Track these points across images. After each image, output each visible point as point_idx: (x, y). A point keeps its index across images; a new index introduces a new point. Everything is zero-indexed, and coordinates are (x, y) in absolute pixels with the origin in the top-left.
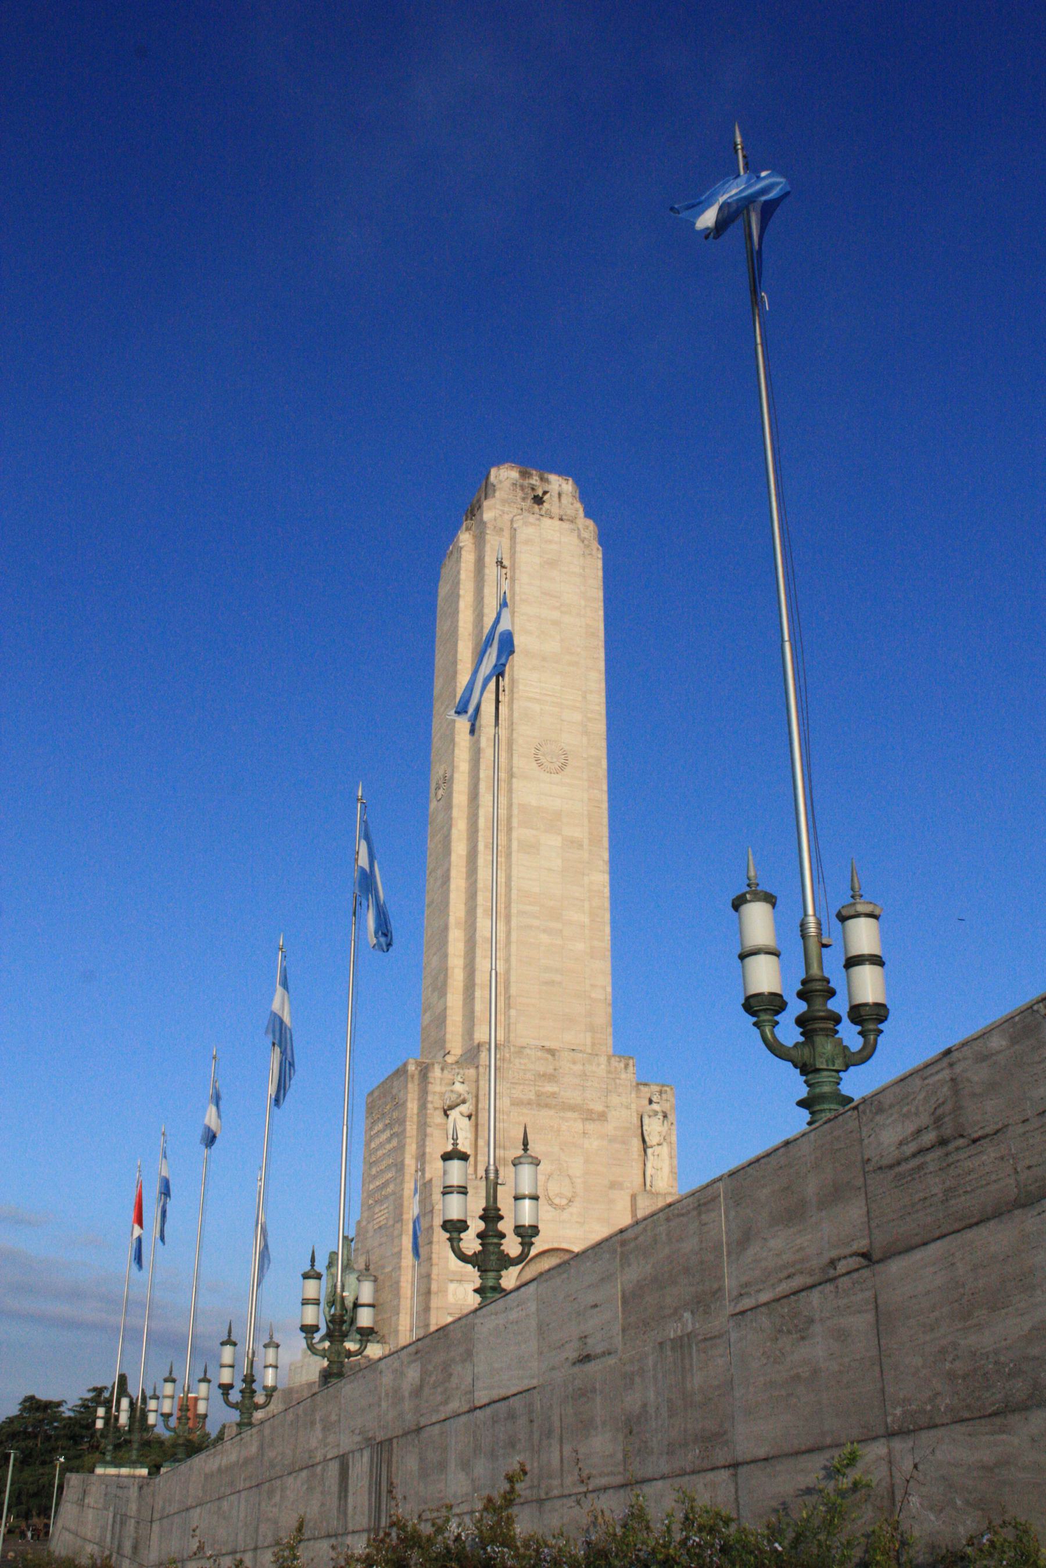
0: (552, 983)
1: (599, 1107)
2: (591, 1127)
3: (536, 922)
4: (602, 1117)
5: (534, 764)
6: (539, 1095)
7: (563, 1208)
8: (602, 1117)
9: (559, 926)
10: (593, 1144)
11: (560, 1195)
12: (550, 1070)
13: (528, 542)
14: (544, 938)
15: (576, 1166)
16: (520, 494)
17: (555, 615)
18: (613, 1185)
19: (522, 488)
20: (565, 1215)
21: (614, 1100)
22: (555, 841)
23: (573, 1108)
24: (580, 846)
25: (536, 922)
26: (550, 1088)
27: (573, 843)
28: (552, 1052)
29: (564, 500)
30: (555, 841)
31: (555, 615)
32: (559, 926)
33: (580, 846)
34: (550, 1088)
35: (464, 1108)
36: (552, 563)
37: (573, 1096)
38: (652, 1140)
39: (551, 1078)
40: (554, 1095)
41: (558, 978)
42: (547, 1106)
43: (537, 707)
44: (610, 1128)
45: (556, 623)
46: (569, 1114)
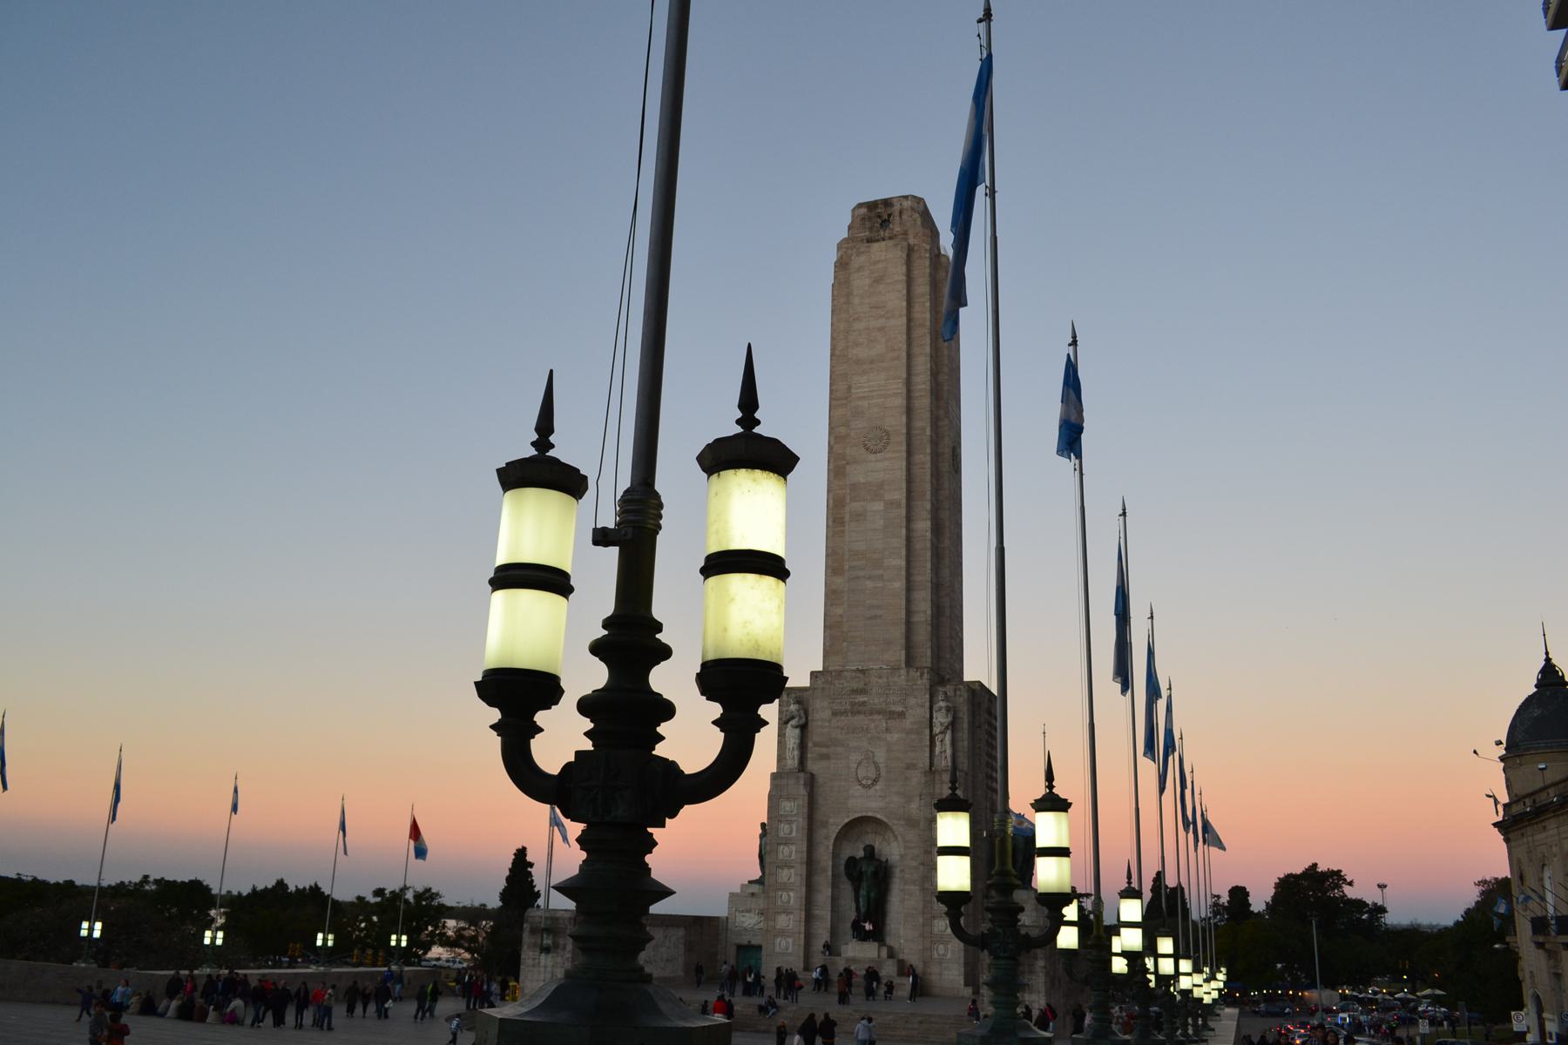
0: (875, 617)
1: (899, 709)
2: (892, 723)
3: (862, 573)
4: (902, 715)
5: (863, 450)
6: (853, 704)
7: (869, 787)
9: (880, 572)
10: (894, 737)
11: (867, 778)
12: (861, 685)
13: (860, 269)
14: (869, 584)
15: (881, 756)
16: (868, 224)
17: (881, 322)
18: (910, 767)
19: (870, 218)
20: (872, 791)
21: (912, 701)
22: (878, 506)
23: (879, 713)
24: (899, 506)
25: (862, 573)
26: (861, 699)
27: (891, 504)
28: (863, 671)
29: (905, 217)
31: (881, 322)
32: (880, 572)
33: (899, 506)
34: (861, 699)
35: (793, 722)
36: (878, 281)
37: (875, 700)
38: (937, 730)
39: (863, 691)
40: (864, 703)
41: (879, 612)
42: (859, 712)
43: (865, 403)
44: (908, 723)
45: (881, 329)
46: (875, 717)
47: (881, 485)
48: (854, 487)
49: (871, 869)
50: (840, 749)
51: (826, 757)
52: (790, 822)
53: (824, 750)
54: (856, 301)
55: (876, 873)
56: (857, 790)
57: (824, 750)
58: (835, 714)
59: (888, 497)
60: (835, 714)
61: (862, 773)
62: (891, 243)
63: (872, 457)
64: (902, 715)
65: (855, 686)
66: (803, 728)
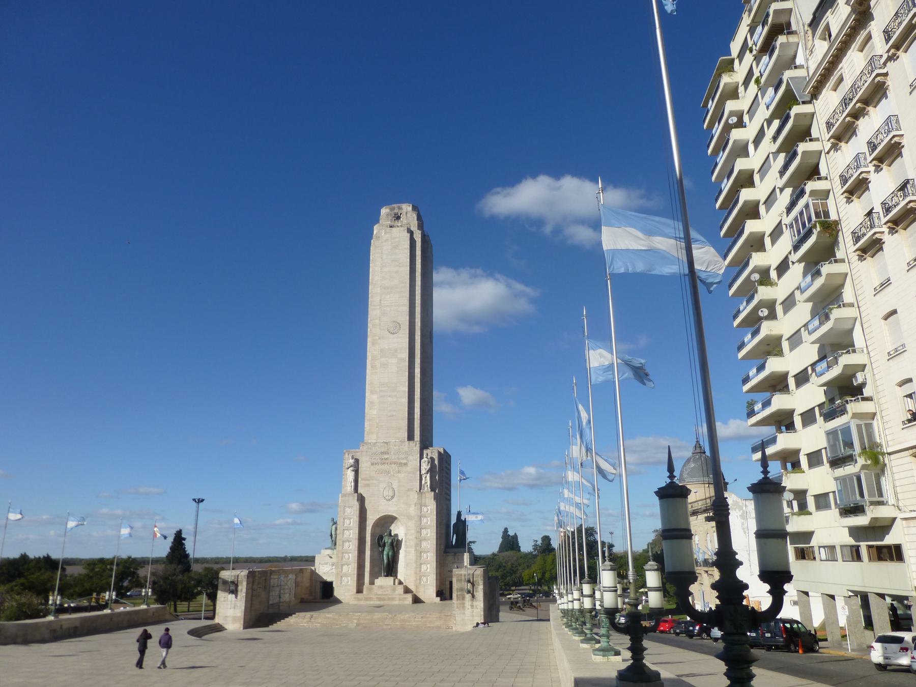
1: (405, 461)
8: (406, 464)
10: (402, 475)
12: (385, 450)
13: (386, 241)
14: (389, 399)
15: (395, 485)
18: (410, 490)
21: (410, 458)
22: (395, 361)
26: (386, 456)
28: (387, 443)
30: (395, 361)
34: (386, 456)
37: (392, 457)
38: (423, 472)
44: (409, 468)
45: (397, 272)
47: (396, 351)
48: (382, 350)
49: (390, 541)
50: (375, 481)
51: (368, 485)
52: (350, 519)
53: (367, 482)
54: (384, 257)
55: (392, 543)
56: (383, 502)
57: (367, 482)
58: (372, 464)
59: (399, 356)
60: (372, 464)
61: (386, 493)
62: (402, 229)
63: (392, 336)
64: (406, 464)
65: (383, 450)
66: (356, 472)
